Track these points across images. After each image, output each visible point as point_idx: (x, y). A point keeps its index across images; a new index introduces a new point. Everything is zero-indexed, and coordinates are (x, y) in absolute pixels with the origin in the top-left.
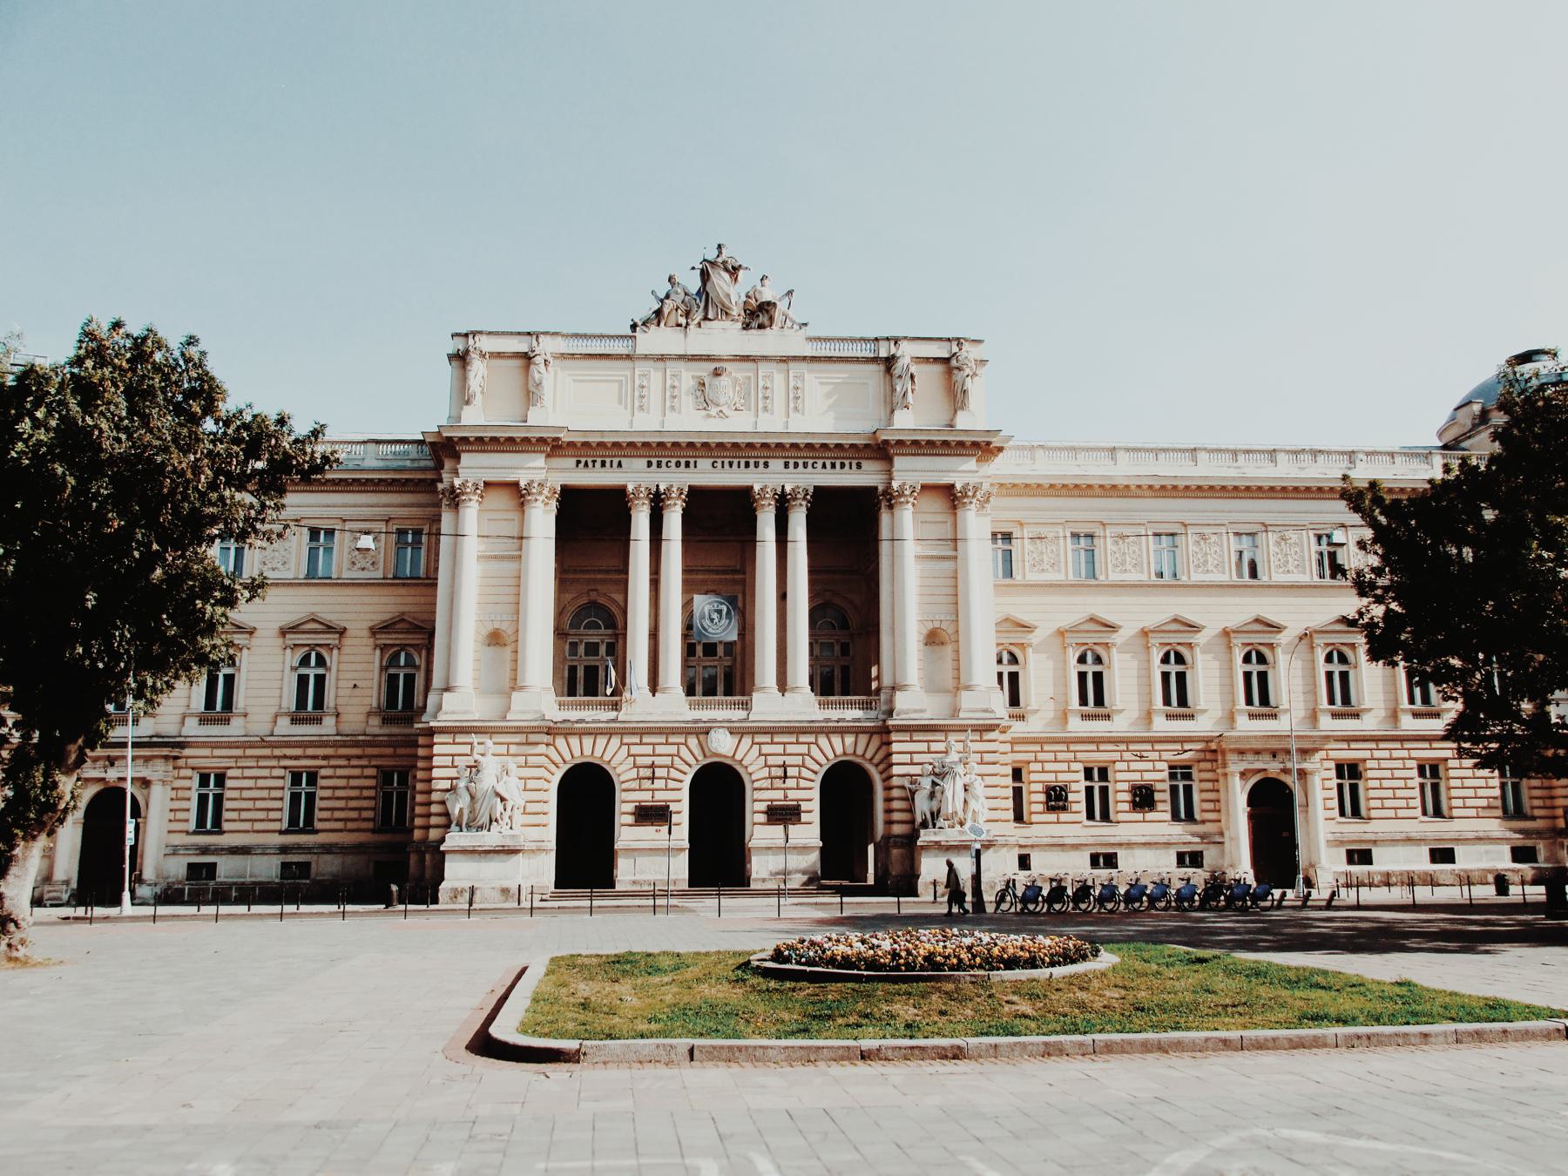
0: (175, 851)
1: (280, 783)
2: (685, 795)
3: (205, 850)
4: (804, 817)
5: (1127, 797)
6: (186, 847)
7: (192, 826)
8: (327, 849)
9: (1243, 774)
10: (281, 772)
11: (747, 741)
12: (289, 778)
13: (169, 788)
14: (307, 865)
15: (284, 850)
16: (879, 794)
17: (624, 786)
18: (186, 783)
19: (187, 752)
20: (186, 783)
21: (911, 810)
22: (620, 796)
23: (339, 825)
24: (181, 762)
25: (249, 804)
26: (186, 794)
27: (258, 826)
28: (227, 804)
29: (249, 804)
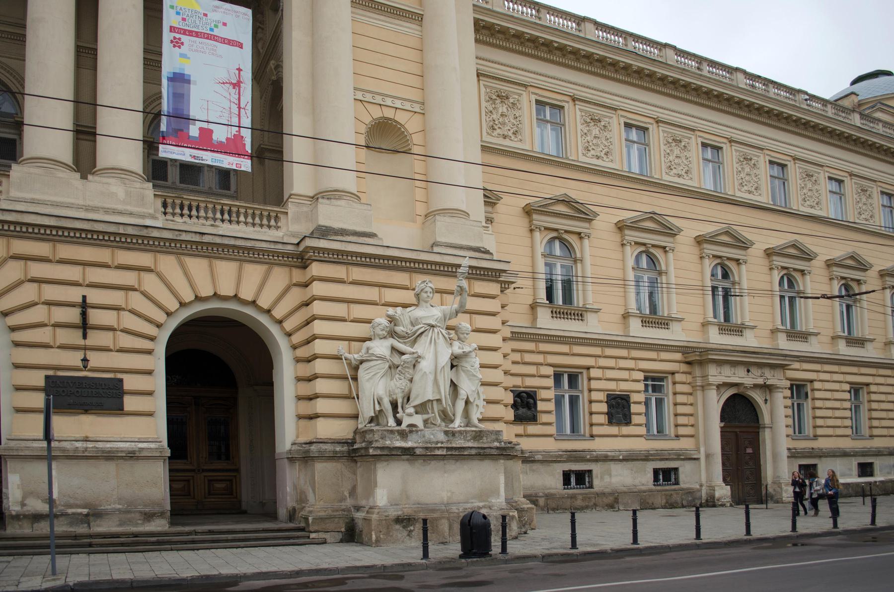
5: (604, 408)
9: (719, 387)
16: (286, 373)
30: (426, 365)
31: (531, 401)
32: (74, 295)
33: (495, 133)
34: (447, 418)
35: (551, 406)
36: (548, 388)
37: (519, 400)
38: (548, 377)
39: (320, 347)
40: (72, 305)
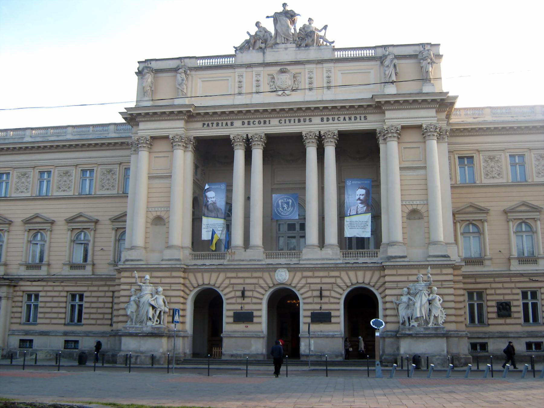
0: (13, 333)
1: (64, 299)
2: (264, 307)
3: (27, 333)
4: (333, 320)
6: (18, 331)
7: (24, 320)
8: (87, 334)
10: (65, 294)
11: (299, 275)
12: (70, 297)
13: (10, 301)
14: (77, 342)
15: (65, 334)
17: (229, 301)
18: (20, 299)
19: (21, 283)
20: (20, 299)
21: (397, 316)
22: (225, 307)
23: (93, 322)
24: (17, 289)
25: (48, 310)
26: (20, 304)
27: (54, 321)
28: (40, 310)
29: (48, 310)
30: (418, 305)
31: (508, 307)
32: (318, 287)
33: (489, 177)
34: (427, 323)
35: (521, 309)
36: (518, 300)
37: (501, 307)
38: (517, 294)
39: (388, 299)
40: (318, 290)
